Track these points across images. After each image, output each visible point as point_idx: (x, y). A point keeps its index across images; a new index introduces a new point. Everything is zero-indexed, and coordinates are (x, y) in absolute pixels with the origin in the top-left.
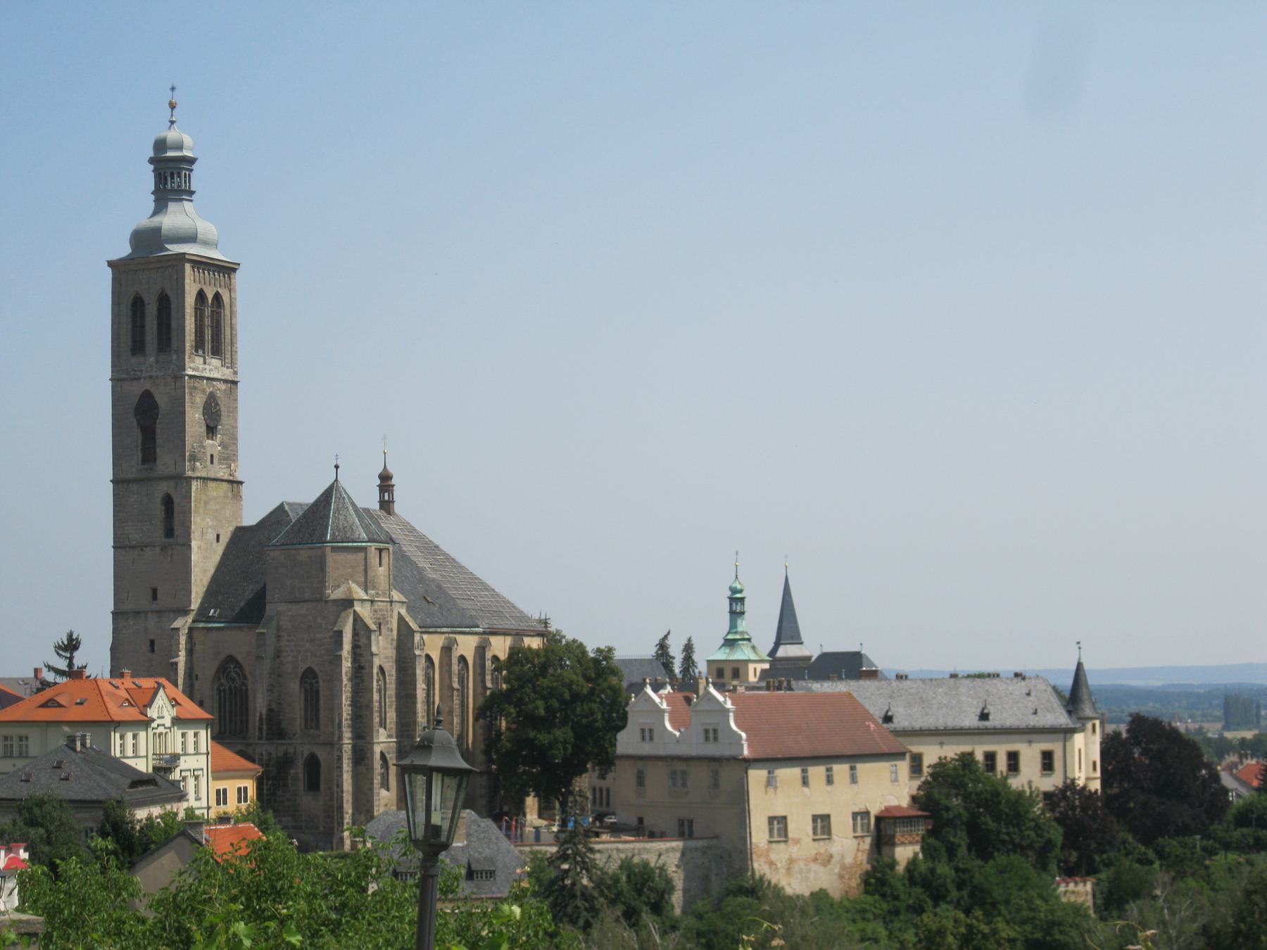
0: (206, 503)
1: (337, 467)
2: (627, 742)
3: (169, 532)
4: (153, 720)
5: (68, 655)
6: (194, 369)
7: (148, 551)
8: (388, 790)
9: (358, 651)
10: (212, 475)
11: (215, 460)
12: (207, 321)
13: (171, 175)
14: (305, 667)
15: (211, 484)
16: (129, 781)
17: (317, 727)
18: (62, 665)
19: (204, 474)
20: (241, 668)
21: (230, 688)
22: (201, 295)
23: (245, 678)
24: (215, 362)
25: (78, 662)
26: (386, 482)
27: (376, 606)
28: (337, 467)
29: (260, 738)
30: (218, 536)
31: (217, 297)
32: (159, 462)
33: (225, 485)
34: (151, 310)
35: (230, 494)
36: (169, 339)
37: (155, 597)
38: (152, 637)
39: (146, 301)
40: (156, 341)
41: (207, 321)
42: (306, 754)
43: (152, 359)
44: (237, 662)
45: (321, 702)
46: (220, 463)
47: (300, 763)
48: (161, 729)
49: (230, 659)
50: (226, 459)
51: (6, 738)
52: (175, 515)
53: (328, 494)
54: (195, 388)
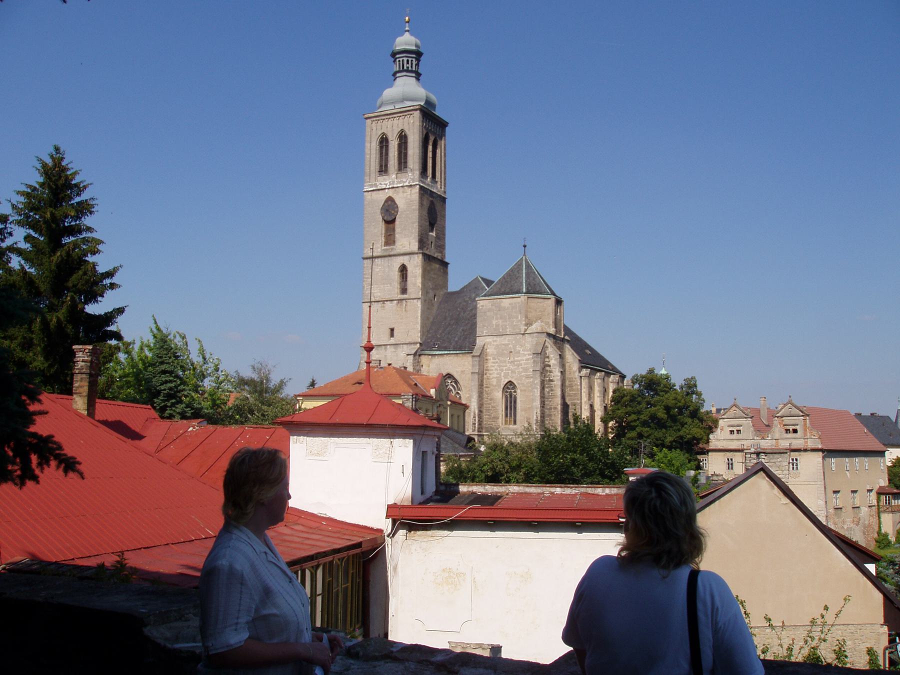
1: (525, 246)
3: (404, 291)
6: (423, 183)
9: (548, 368)
12: (430, 154)
14: (507, 381)
17: (515, 423)
20: (456, 382)
28: (525, 246)
29: (474, 431)
36: (406, 162)
37: (392, 335)
39: (390, 139)
41: (430, 154)
43: (394, 176)
44: (454, 378)
53: (519, 265)
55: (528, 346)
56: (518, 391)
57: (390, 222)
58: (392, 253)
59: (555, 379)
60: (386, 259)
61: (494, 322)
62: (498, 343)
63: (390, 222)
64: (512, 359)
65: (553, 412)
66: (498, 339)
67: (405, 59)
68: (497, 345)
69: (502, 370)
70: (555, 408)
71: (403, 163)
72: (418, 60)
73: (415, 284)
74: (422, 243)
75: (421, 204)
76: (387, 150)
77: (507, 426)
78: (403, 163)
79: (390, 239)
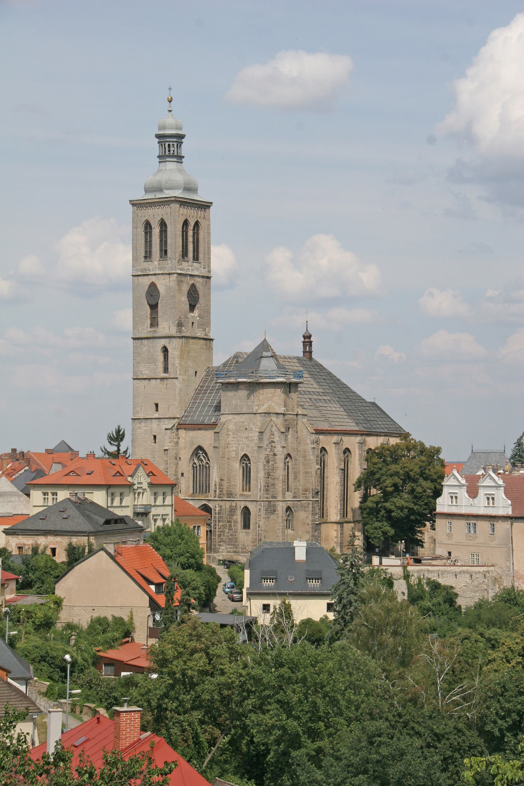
0: (188, 352)
2: (443, 504)
3: (166, 370)
4: (135, 484)
5: (116, 444)
6: (181, 270)
7: (153, 381)
8: (293, 530)
9: (273, 444)
10: (193, 335)
11: (196, 325)
12: (190, 239)
13: (170, 145)
14: (243, 453)
15: (191, 341)
16: (104, 520)
17: (249, 490)
18: (113, 449)
19: (188, 334)
20: (206, 454)
21: (200, 465)
22: (186, 223)
23: (209, 460)
24: (196, 265)
25: (122, 449)
26: (307, 340)
27: (286, 417)
29: (215, 497)
30: (196, 372)
31: (197, 224)
32: (160, 326)
33: (202, 342)
34: (156, 231)
35: (204, 347)
36: (166, 251)
38: (155, 434)
40: (158, 251)
41: (190, 239)
42: (242, 508)
45: (252, 475)
46: (198, 327)
47: (239, 512)
48: (140, 490)
49: (200, 448)
50: (201, 325)
51: (45, 494)
52: (169, 360)
54: (182, 281)
55: (259, 424)
56: (252, 463)
57: (154, 307)
58: (156, 335)
59: (278, 453)
60: (151, 340)
61: (234, 402)
62: (236, 420)
63: (154, 307)
64: (247, 435)
65: (276, 482)
66: (237, 417)
67: (167, 144)
68: (236, 423)
69: (239, 444)
70: (278, 478)
71: (164, 252)
72: (180, 144)
73: (173, 365)
74: (180, 325)
75: (180, 290)
76: (151, 236)
77: (243, 493)
78: (164, 252)
79: (154, 323)
